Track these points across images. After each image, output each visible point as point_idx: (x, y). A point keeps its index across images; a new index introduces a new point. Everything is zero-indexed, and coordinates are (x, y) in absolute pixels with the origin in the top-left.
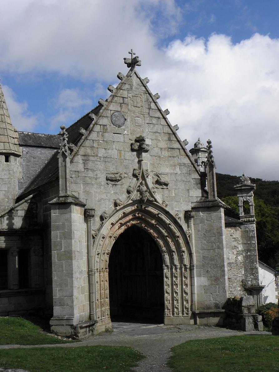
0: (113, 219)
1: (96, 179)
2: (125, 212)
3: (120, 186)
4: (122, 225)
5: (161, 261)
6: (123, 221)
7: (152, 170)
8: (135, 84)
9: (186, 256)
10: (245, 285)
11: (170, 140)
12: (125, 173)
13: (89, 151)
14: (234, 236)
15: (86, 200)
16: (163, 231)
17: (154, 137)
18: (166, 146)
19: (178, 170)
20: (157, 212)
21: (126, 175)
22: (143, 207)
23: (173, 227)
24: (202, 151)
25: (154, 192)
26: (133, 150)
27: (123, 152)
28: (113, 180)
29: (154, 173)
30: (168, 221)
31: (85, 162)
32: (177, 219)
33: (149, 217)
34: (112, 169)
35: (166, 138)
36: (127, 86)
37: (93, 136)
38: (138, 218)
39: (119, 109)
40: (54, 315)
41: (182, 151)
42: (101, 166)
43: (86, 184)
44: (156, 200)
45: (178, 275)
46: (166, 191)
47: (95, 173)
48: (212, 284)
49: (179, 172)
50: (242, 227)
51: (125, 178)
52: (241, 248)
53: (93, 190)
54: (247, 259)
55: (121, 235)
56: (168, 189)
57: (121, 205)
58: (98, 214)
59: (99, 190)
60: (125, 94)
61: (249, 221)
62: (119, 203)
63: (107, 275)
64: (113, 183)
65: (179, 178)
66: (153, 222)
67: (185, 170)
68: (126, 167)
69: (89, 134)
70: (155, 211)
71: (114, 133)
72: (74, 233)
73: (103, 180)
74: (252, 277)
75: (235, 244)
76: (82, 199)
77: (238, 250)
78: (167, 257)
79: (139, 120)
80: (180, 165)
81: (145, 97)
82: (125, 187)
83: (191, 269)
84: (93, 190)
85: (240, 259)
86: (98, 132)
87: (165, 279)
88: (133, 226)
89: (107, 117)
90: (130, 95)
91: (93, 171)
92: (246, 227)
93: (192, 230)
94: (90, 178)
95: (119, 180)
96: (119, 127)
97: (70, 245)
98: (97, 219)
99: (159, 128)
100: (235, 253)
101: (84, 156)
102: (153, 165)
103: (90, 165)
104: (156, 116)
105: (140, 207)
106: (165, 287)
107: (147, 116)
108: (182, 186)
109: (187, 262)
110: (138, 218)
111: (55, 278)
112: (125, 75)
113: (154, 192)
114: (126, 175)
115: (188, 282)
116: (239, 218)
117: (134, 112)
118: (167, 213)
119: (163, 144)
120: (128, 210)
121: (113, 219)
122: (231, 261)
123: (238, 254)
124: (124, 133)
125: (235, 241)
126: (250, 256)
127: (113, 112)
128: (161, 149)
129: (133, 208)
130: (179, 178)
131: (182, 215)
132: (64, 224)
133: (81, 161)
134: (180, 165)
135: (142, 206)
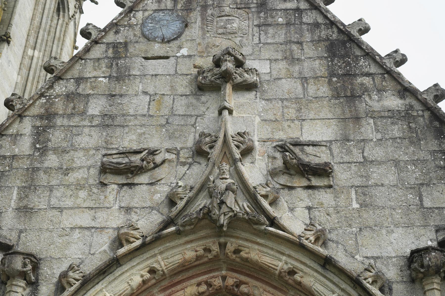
2: (156, 265)
3: (145, 188)
7: (270, 136)
12: (168, 151)
15: (21, 232)
20: (286, 263)
21: (168, 156)
22: (230, 248)
25: (265, 197)
29: (275, 144)
32: (364, 282)
33: (264, 286)
44: (273, 222)
47: (67, 157)
51: (166, 165)
56: (330, 187)
57: (132, 239)
62: (126, 234)
64: (121, 180)
71: (146, 58)
105: (215, 248)
113: (265, 197)
114: (168, 156)
120: (171, 260)
124: (178, 55)
127: (151, 12)
129: (190, 254)
135: (223, 246)
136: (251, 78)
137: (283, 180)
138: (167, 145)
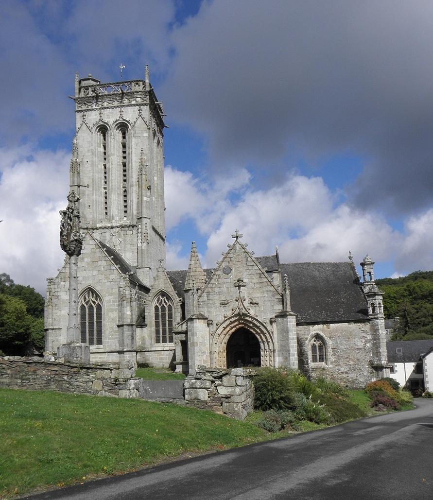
0: (224, 325)
1: (214, 304)
4: (232, 328)
5: (259, 347)
6: (232, 325)
8: (238, 249)
9: (271, 344)
10: (373, 364)
11: (260, 277)
13: (210, 290)
14: (363, 329)
16: (258, 330)
17: (249, 277)
18: (258, 281)
19: (266, 294)
23: (262, 328)
24: (367, 264)
26: (235, 286)
27: (229, 288)
28: (223, 304)
30: (258, 325)
31: (208, 296)
34: (223, 298)
35: (258, 276)
36: (233, 251)
37: (213, 281)
38: (242, 323)
39: (228, 264)
40: (190, 372)
41: (269, 283)
42: (217, 297)
43: (208, 307)
45: (268, 355)
46: (257, 308)
48: (284, 361)
49: (267, 296)
50: (371, 322)
52: (369, 337)
53: (212, 310)
54: (374, 345)
55: (233, 333)
58: (215, 322)
59: (215, 310)
60: (231, 255)
61: (374, 318)
63: (225, 354)
65: (266, 299)
66: (251, 325)
67: (270, 294)
68: (232, 296)
69: (210, 281)
70: (250, 320)
72: (196, 333)
73: (218, 305)
74: (377, 358)
75: (364, 334)
76: (206, 315)
77: (366, 339)
78: (262, 344)
79: (241, 269)
80: (267, 291)
81: (243, 255)
82: (231, 307)
83: (274, 352)
84: (212, 310)
85: (368, 346)
86: (215, 279)
87: (261, 357)
88: (241, 328)
89: (220, 270)
90: (234, 255)
91: (212, 300)
92: (373, 323)
93: (274, 329)
94: (211, 304)
95: (227, 304)
96: (228, 274)
97: (194, 339)
98: (215, 325)
99: (253, 271)
100: (364, 341)
101: (207, 292)
102: (249, 293)
103: (211, 297)
104: (252, 264)
106: (262, 362)
107: (246, 265)
108: (268, 304)
109: (271, 348)
110: (242, 323)
111: (189, 355)
112: (232, 245)
115: (272, 359)
116: (368, 316)
117: (237, 265)
118: (257, 320)
119: (256, 280)
121: (224, 325)
122: (360, 347)
123: (367, 342)
125: (364, 332)
126: (376, 343)
128: (255, 283)
129: (236, 318)
130: (266, 299)
131: (268, 321)
132: (192, 329)
133: (206, 296)
134: (267, 291)
136: (244, 284)
137: (251, 305)
138: (231, 298)
